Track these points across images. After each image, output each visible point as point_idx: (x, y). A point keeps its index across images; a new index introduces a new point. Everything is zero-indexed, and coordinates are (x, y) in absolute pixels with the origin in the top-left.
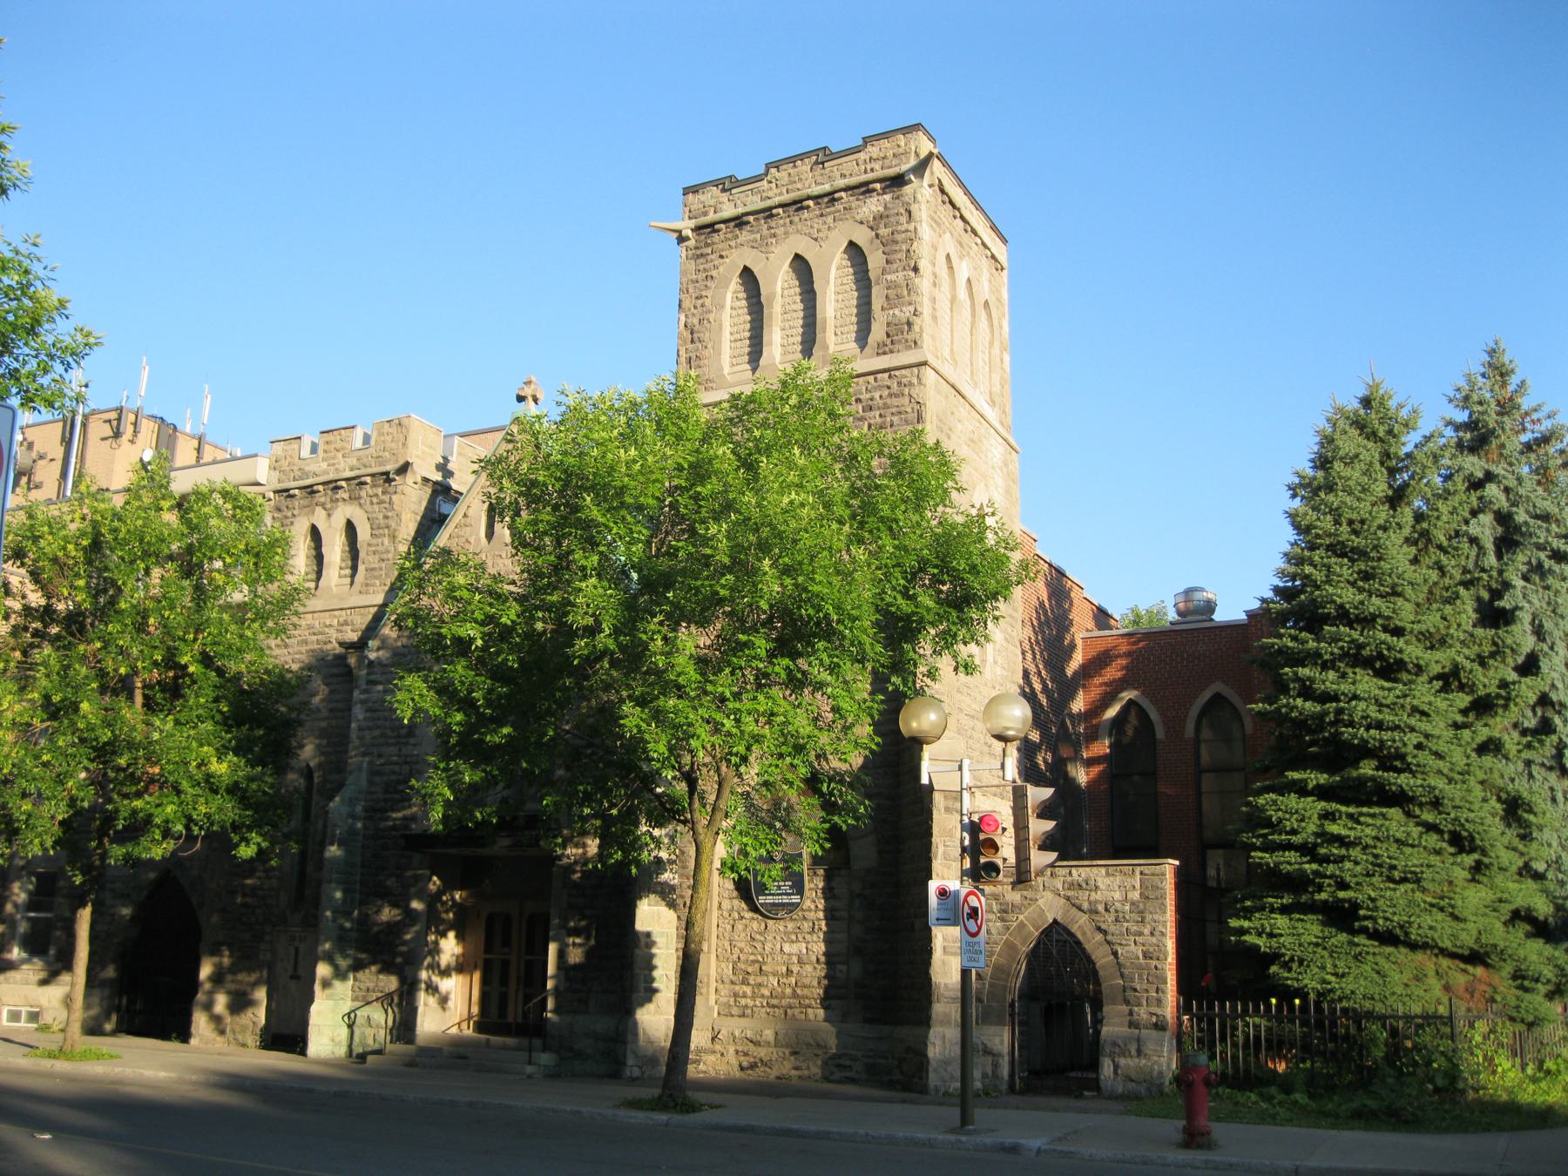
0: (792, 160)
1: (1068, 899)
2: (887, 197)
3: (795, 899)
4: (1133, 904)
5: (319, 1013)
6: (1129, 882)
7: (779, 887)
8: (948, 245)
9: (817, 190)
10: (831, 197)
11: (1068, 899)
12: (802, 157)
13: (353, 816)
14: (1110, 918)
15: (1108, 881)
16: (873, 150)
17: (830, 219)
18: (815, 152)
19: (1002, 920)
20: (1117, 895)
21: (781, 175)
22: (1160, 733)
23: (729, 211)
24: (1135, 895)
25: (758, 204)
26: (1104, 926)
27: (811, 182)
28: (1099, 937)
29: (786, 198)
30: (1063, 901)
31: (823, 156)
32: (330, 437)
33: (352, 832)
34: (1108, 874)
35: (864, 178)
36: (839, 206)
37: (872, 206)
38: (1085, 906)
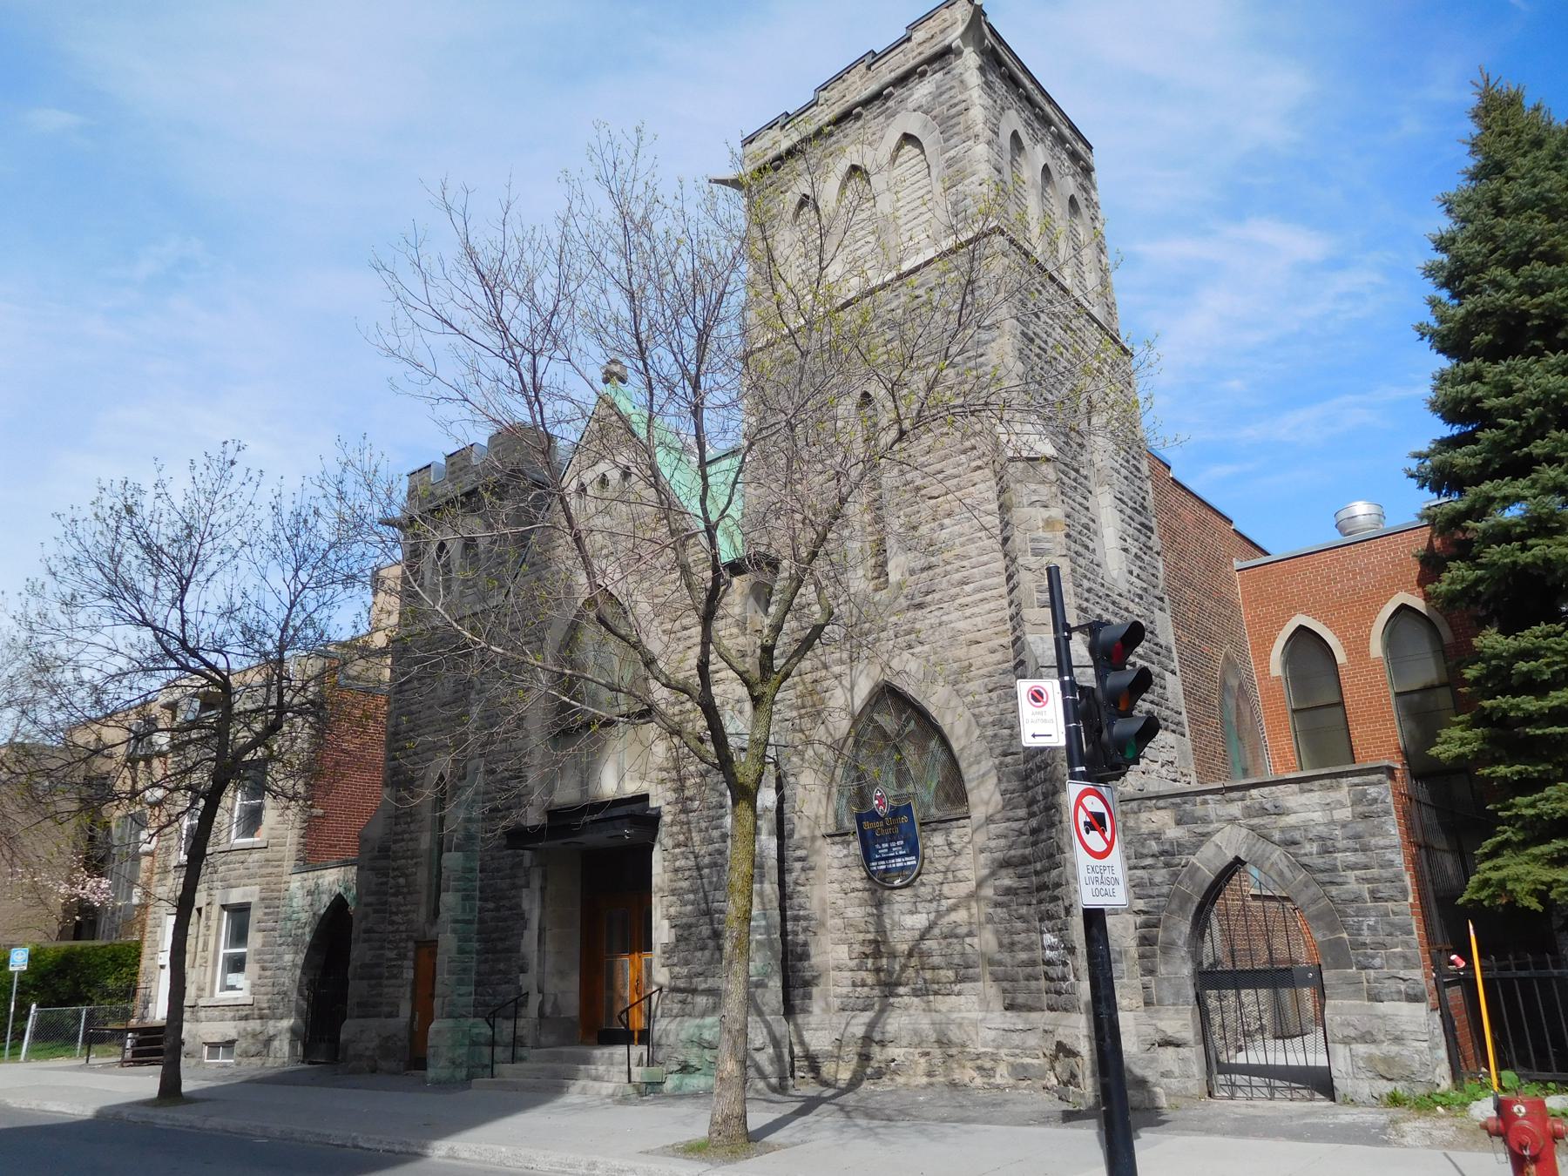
0: (839, 77)
1: (1252, 828)
2: (939, 75)
3: (911, 861)
4: (1344, 826)
5: (438, 1032)
6: (1333, 796)
7: (890, 849)
8: (1014, 120)
9: (865, 94)
10: (878, 96)
11: (1252, 828)
12: (848, 70)
13: (469, 820)
14: (1315, 848)
15: (1304, 798)
16: (919, 36)
17: (882, 119)
18: (861, 60)
19: (1167, 865)
20: (1318, 816)
21: (834, 94)
22: (1341, 657)
23: (785, 145)
24: (1345, 814)
25: (811, 128)
26: (1305, 860)
27: (860, 87)
28: (1302, 876)
29: (837, 110)
30: (1244, 831)
31: (873, 58)
32: (455, 459)
33: (469, 837)
34: (1302, 791)
35: (911, 63)
36: (891, 103)
37: (922, 91)
38: (1277, 836)
